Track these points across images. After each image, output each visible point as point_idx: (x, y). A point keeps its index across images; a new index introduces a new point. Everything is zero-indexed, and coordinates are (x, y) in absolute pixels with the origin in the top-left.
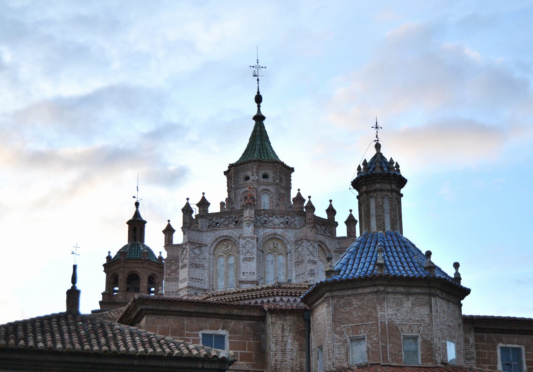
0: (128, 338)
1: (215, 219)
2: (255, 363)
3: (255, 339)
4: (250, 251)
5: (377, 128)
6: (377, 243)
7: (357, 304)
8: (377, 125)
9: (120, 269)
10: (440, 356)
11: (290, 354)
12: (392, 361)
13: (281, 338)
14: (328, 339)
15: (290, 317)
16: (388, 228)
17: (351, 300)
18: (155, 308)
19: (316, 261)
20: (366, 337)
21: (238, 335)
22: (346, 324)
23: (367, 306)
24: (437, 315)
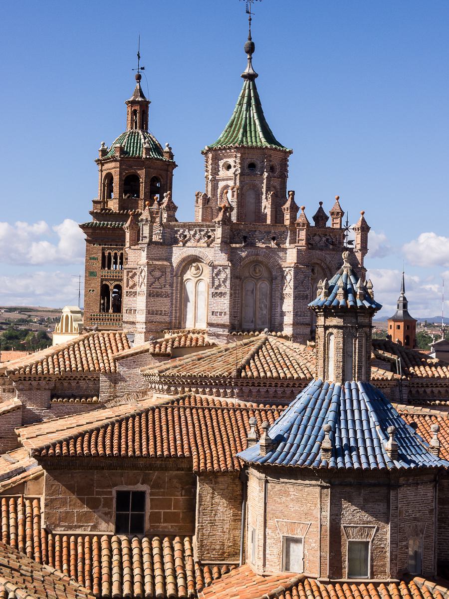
1: (182, 230)
3: (183, 494)
7: (294, 495)
8: (347, 226)
10: (395, 568)
15: (223, 479)
21: (162, 490)
23: (306, 500)
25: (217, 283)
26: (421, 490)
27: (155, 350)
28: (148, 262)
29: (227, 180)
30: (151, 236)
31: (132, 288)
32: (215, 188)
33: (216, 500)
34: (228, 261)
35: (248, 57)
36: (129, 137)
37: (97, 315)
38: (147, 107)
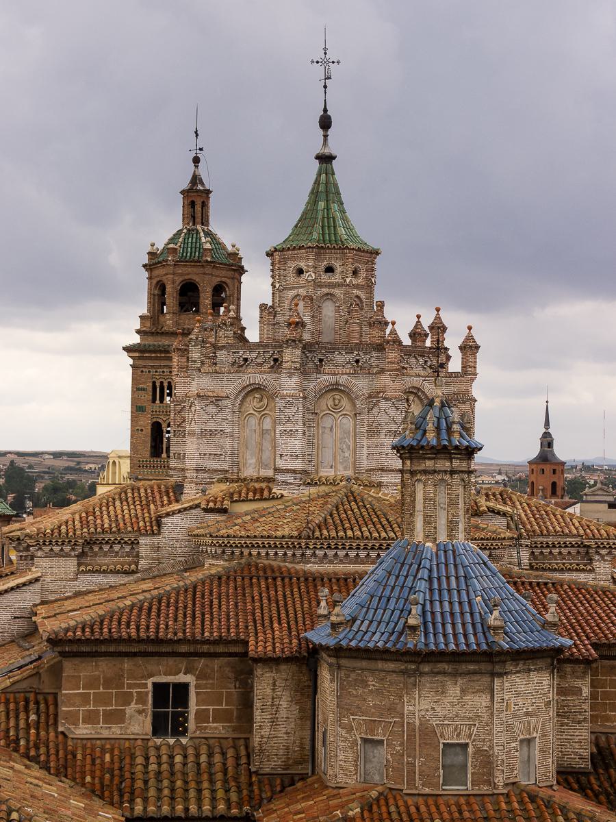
3: (237, 686)
9: (168, 276)
11: (285, 726)
12: (423, 785)
13: (270, 700)
16: (442, 538)
18: (75, 651)
23: (389, 692)
26: (535, 677)
27: (208, 505)
31: (179, 426)
33: (278, 693)
37: (146, 461)
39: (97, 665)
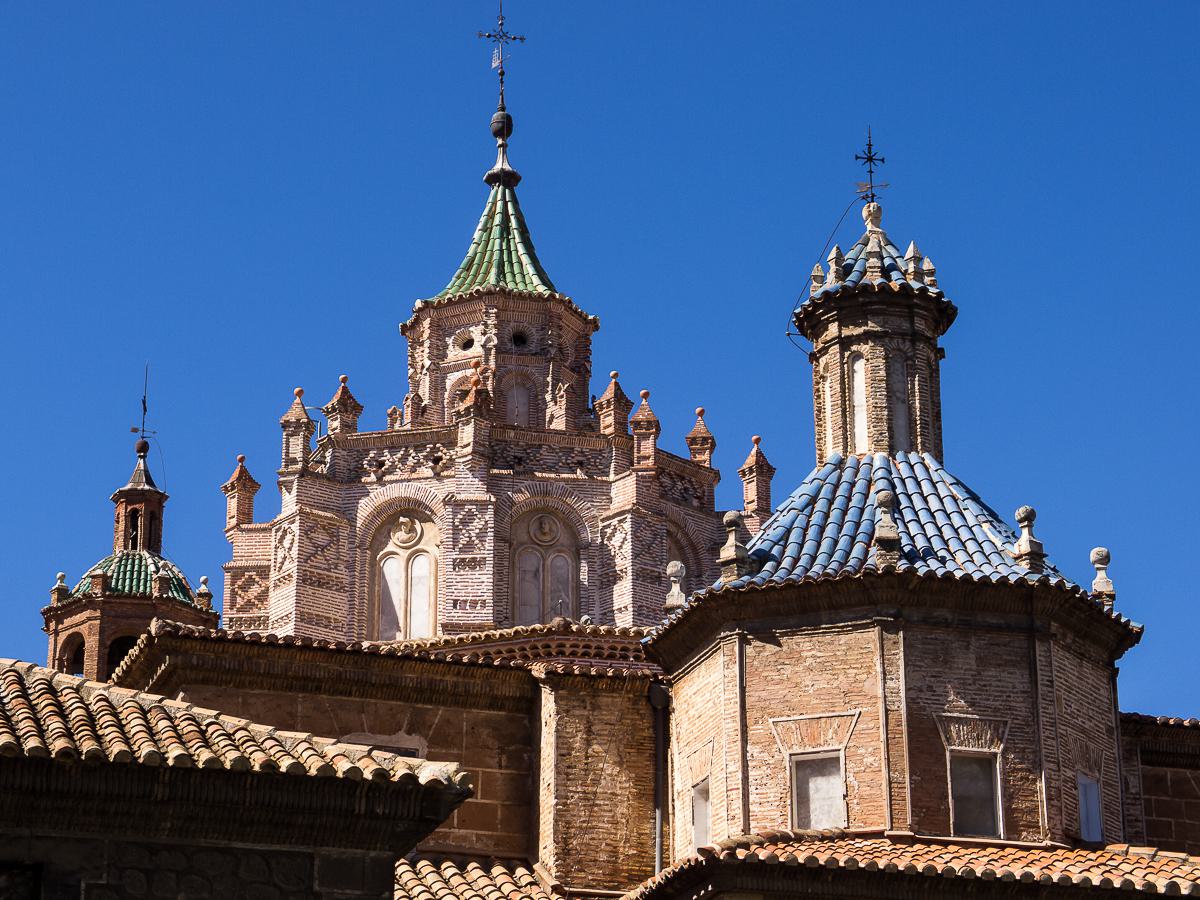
0: (134, 725)
2: (503, 834)
3: (503, 764)
4: (473, 539)
5: (870, 159)
6: (870, 483)
7: (813, 656)
8: (870, 152)
10: (1058, 817)
14: (728, 759)
15: (610, 699)
17: (798, 644)
19: (659, 573)
20: (842, 754)
22: (782, 716)
23: (844, 662)
24: (1050, 694)
25: (463, 541)
28: (301, 510)
29: (465, 366)
30: (306, 461)
32: (438, 387)
34: (488, 492)
35: (500, 142)
36: (120, 561)
38: (161, 506)
39: (245, 703)
